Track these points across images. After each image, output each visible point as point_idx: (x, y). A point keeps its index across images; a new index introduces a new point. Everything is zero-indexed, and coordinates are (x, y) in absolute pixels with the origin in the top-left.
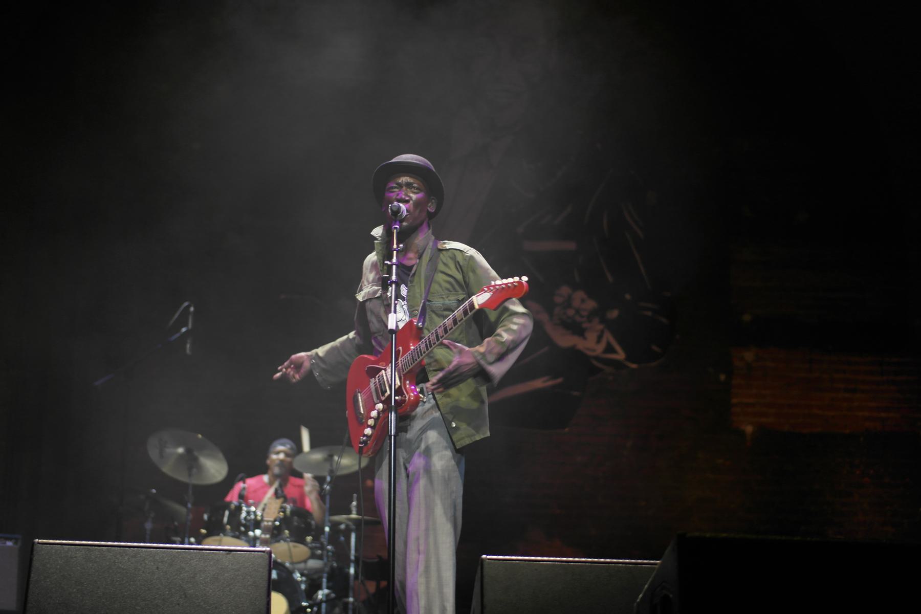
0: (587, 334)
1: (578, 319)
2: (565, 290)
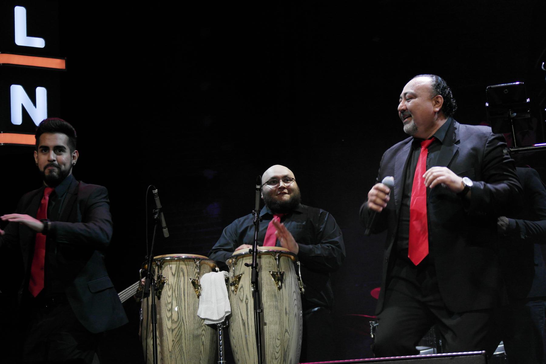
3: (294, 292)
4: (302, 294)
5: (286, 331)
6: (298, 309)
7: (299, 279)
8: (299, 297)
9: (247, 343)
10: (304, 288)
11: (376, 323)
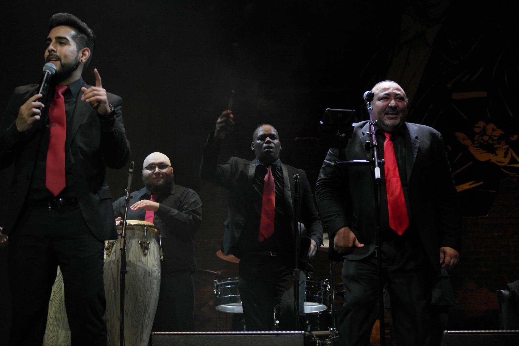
0: (498, 152)
1: (491, 142)
2: (481, 124)
4: (161, 260)
5: (148, 290)
6: (159, 272)
7: (160, 249)
9: (115, 298)
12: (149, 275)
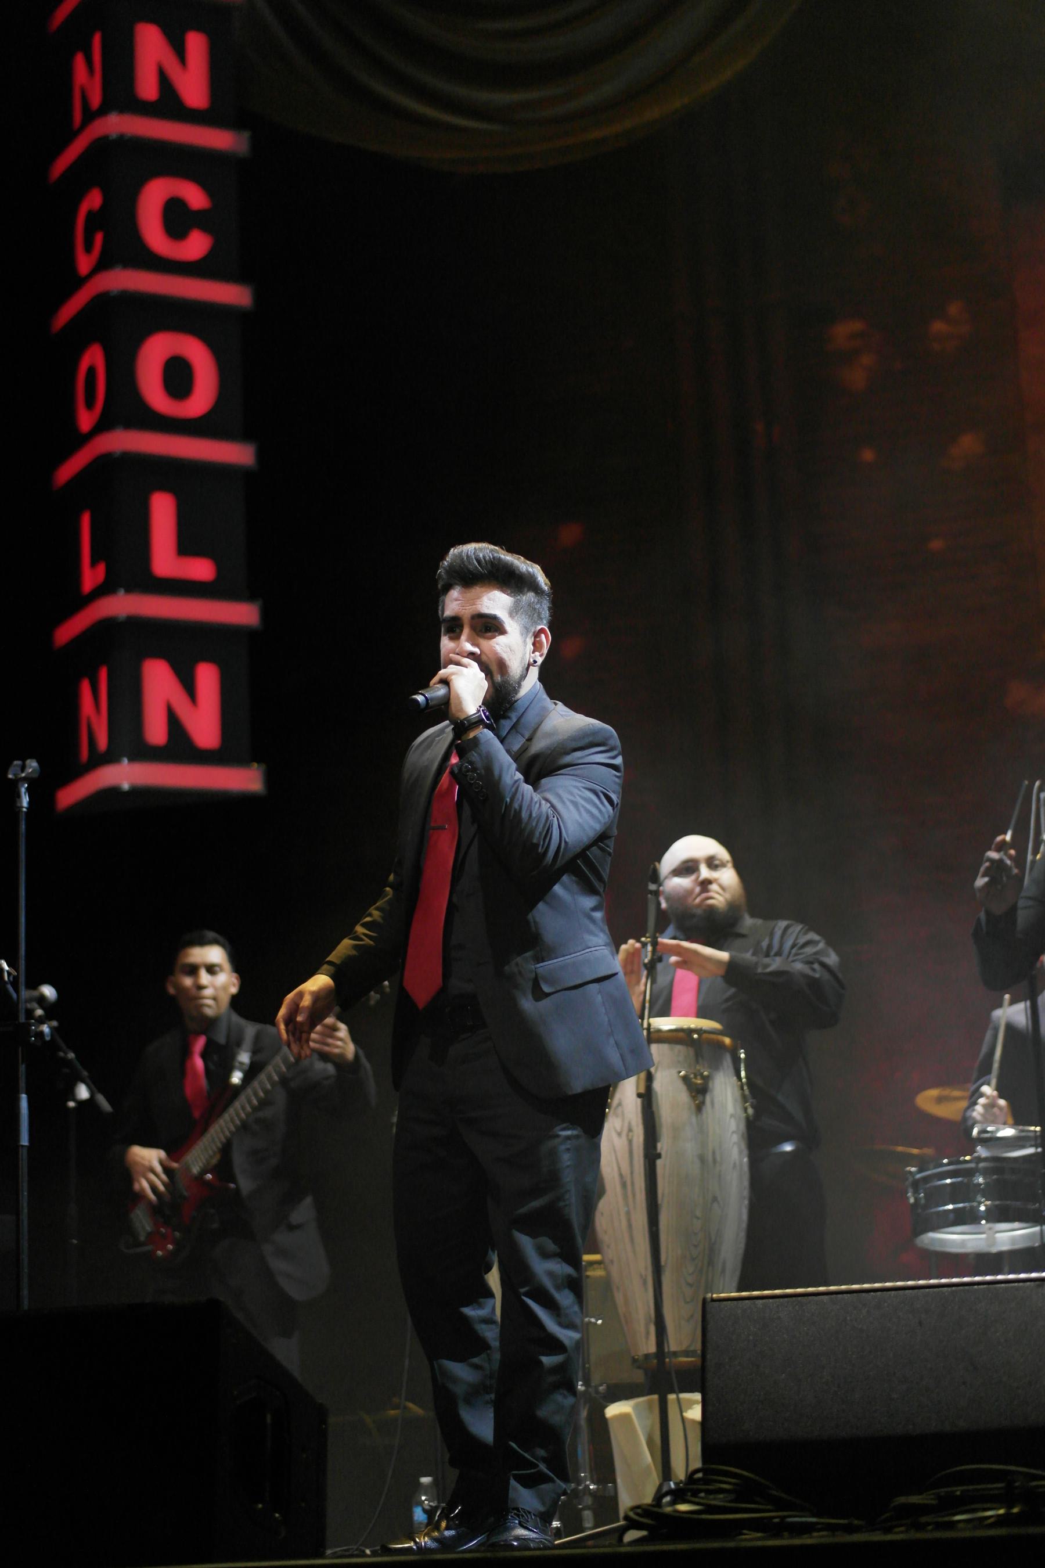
3: (732, 1116)
4: (748, 1119)
5: (715, 1199)
6: (740, 1152)
7: (742, 1088)
8: (742, 1126)
10: (752, 1106)
11: (920, 1171)
12: (715, 1161)
